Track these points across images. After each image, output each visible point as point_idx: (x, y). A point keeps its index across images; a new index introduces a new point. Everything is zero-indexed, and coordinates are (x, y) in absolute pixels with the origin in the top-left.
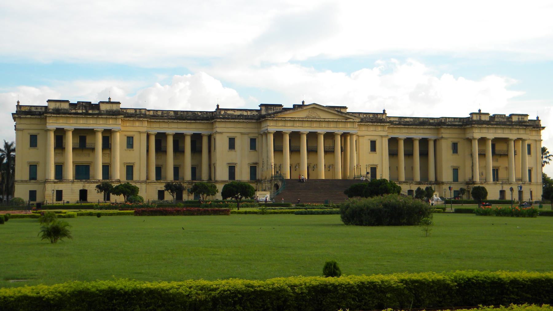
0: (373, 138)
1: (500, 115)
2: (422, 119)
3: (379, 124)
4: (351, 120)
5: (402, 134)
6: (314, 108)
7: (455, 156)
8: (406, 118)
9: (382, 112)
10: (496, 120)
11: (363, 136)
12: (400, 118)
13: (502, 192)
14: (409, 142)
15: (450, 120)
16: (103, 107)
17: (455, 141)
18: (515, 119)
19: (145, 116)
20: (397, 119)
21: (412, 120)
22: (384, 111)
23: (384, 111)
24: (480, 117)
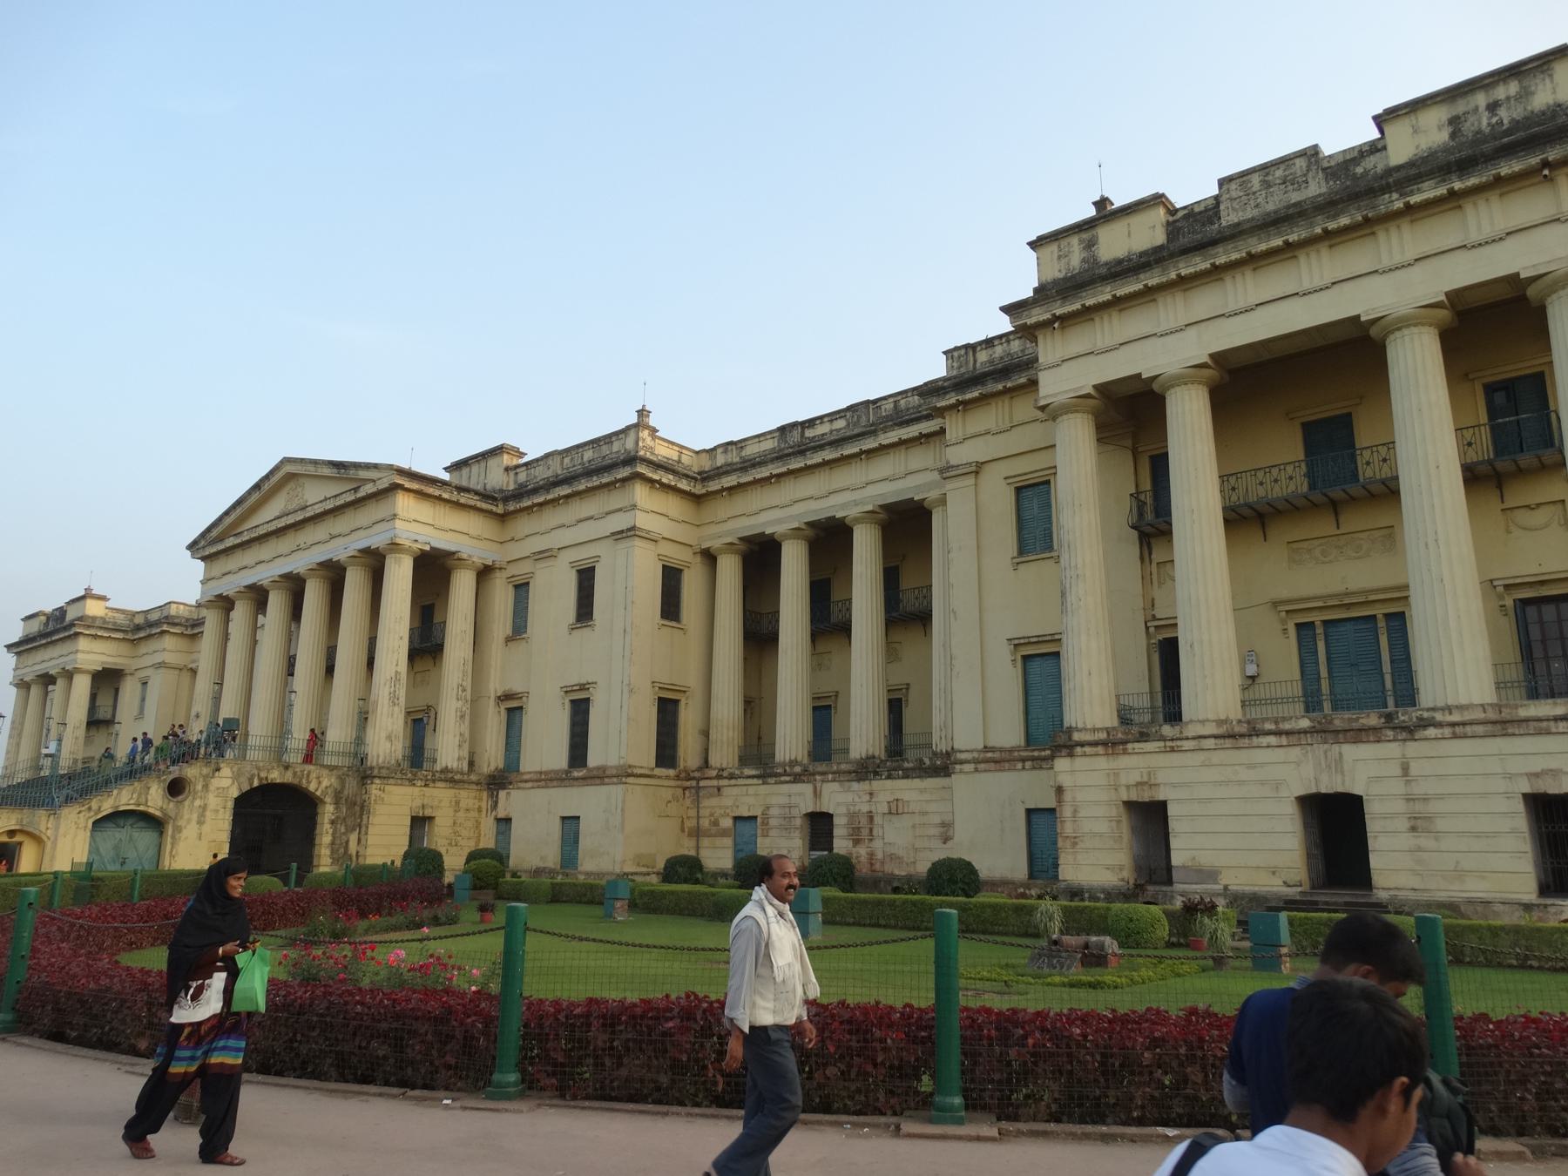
0: (582, 554)
1: (1265, 168)
2: (888, 407)
3: (595, 481)
4: (369, 489)
5: (783, 510)
6: (291, 477)
7: (1036, 571)
8: (811, 423)
9: (634, 419)
10: (1229, 217)
11: (544, 555)
12: (783, 430)
13: (1336, 825)
14: (829, 540)
15: (999, 350)
16: (70, 617)
17: (1027, 467)
18: (1402, 148)
19: (170, 620)
20: (769, 445)
21: (841, 424)
22: (643, 413)
23: (643, 413)
24: (1090, 244)
